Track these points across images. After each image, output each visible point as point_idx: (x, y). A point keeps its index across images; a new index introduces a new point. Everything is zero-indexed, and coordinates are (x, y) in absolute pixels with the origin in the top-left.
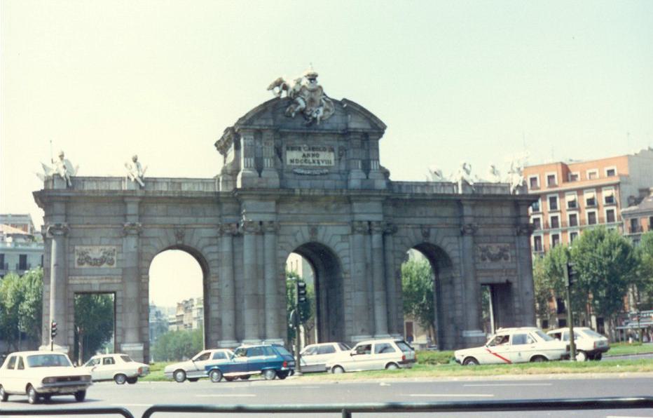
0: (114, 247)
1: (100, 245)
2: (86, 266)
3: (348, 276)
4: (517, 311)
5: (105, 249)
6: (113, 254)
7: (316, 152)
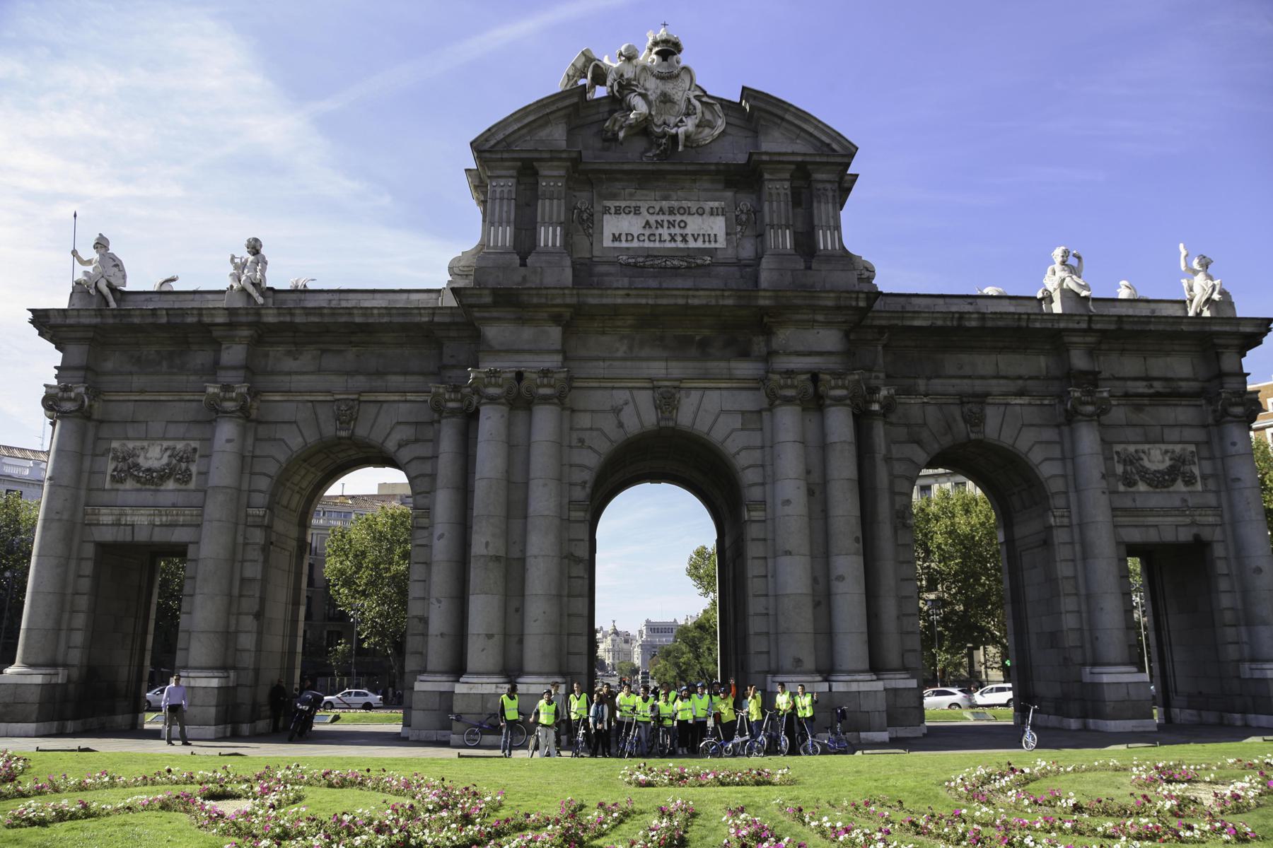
0: (194, 444)
1: (164, 439)
2: (129, 484)
3: (756, 515)
4: (1228, 616)
5: (175, 448)
6: (189, 461)
7: (678, 218)
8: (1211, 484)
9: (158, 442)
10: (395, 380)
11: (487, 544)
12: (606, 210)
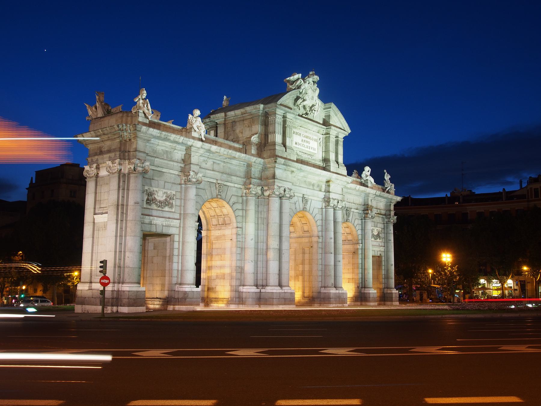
0: (174, 193)
5: (167, 193)
7: (308, 140)
8: (383, 241)
9: (161, 189)
10: (234, 178)
11: (278, 244)
12: (294, 133)
